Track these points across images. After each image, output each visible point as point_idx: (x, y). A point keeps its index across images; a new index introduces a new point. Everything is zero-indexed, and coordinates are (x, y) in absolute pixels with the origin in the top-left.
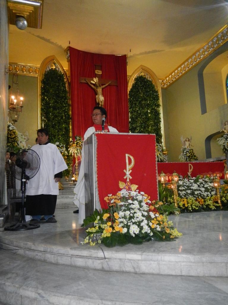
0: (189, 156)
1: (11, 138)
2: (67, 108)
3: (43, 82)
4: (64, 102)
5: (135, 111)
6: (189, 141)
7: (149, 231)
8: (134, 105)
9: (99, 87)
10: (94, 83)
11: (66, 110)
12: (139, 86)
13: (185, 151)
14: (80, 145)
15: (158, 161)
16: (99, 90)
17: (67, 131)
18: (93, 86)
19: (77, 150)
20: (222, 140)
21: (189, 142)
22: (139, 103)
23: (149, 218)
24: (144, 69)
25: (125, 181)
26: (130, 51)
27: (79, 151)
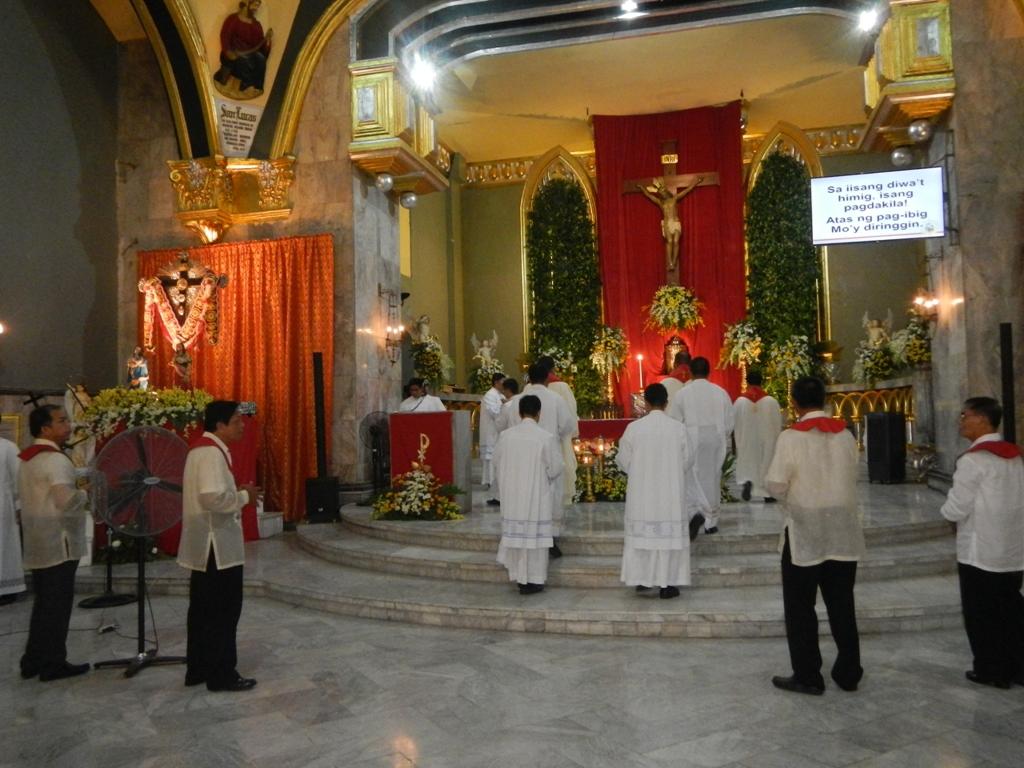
0: (871, 369)
1: (429, 367)
2: (588, 262)
3: (530, 215)
4: (580, 250)
5: (760, 249)
6: (879, 326)
7: (417, 511)
8: (757, 231)
9: (669, 200)
10: (655, 191)
11: (588, 268)
12: (768, 181)
13: (862, 356)
14: (614, 346)
15: (793, 380)
16: (669, 207)
17: (593, 312)
18: (654, 198)
19: (606, 359)
20: (901, 337)
21: (881, 330)
22: (770, 226)
23: (421, 499)
24: (786, 131)
25: (418, 461)
26: (742, 95)
27: (610, 360)
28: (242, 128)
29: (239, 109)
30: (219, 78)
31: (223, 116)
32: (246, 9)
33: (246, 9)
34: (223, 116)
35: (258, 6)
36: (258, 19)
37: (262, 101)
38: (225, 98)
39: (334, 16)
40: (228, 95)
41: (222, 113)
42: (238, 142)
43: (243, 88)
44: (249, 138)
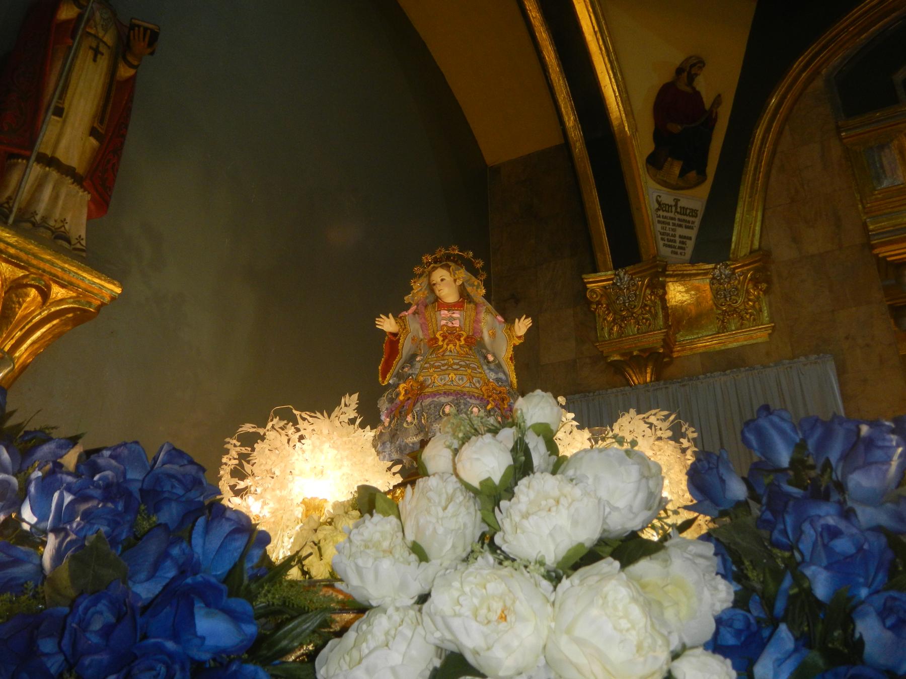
28: (680, 226)
29: (677, 201)
30: (654, 162)
31: (658, 210)
32: (685, 74)
33: (685, 74)
34: (658, 210)
35: (701, 68)
36: (698, 89)
37: (704, 190)
38: (659, 187)
39: (802, 71)
40: (664, 184)
41: (657, 206)
42: (677, 244)
43: (683, 173)
44: (690, 238)
